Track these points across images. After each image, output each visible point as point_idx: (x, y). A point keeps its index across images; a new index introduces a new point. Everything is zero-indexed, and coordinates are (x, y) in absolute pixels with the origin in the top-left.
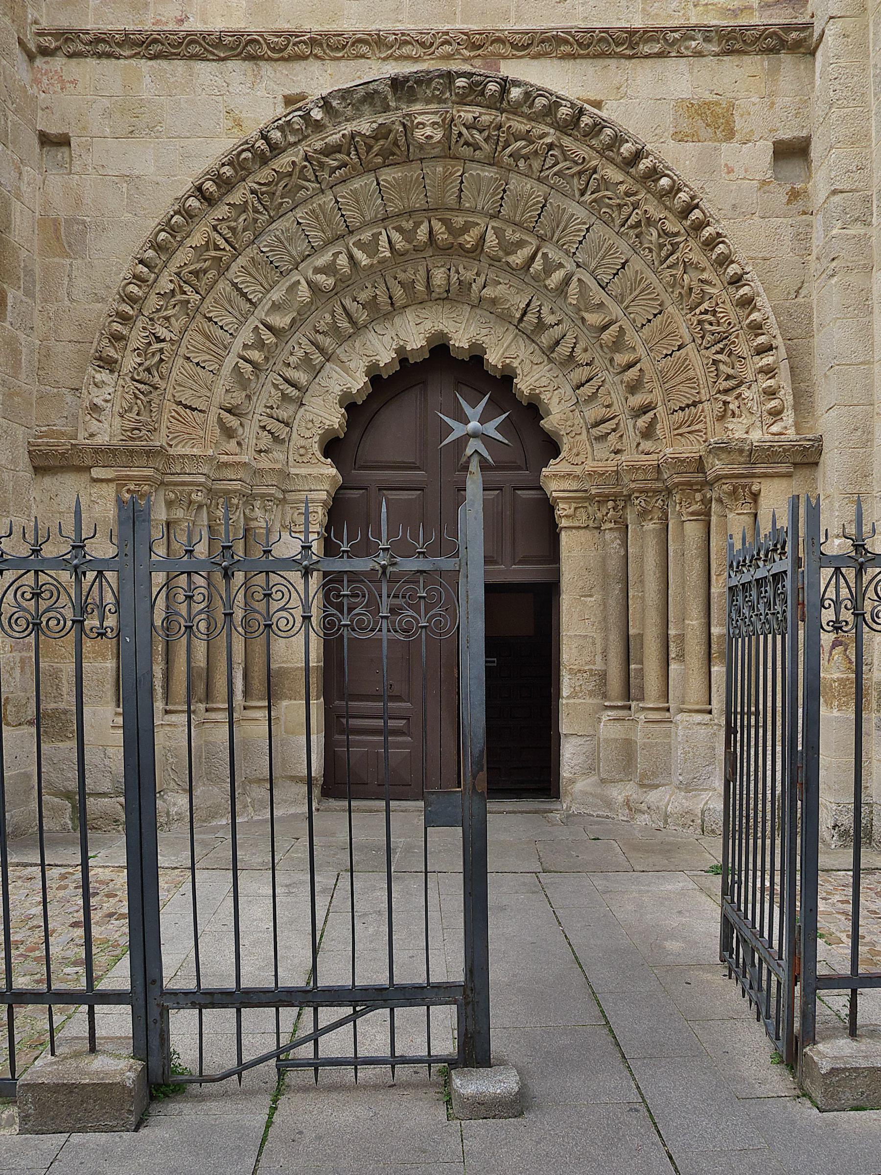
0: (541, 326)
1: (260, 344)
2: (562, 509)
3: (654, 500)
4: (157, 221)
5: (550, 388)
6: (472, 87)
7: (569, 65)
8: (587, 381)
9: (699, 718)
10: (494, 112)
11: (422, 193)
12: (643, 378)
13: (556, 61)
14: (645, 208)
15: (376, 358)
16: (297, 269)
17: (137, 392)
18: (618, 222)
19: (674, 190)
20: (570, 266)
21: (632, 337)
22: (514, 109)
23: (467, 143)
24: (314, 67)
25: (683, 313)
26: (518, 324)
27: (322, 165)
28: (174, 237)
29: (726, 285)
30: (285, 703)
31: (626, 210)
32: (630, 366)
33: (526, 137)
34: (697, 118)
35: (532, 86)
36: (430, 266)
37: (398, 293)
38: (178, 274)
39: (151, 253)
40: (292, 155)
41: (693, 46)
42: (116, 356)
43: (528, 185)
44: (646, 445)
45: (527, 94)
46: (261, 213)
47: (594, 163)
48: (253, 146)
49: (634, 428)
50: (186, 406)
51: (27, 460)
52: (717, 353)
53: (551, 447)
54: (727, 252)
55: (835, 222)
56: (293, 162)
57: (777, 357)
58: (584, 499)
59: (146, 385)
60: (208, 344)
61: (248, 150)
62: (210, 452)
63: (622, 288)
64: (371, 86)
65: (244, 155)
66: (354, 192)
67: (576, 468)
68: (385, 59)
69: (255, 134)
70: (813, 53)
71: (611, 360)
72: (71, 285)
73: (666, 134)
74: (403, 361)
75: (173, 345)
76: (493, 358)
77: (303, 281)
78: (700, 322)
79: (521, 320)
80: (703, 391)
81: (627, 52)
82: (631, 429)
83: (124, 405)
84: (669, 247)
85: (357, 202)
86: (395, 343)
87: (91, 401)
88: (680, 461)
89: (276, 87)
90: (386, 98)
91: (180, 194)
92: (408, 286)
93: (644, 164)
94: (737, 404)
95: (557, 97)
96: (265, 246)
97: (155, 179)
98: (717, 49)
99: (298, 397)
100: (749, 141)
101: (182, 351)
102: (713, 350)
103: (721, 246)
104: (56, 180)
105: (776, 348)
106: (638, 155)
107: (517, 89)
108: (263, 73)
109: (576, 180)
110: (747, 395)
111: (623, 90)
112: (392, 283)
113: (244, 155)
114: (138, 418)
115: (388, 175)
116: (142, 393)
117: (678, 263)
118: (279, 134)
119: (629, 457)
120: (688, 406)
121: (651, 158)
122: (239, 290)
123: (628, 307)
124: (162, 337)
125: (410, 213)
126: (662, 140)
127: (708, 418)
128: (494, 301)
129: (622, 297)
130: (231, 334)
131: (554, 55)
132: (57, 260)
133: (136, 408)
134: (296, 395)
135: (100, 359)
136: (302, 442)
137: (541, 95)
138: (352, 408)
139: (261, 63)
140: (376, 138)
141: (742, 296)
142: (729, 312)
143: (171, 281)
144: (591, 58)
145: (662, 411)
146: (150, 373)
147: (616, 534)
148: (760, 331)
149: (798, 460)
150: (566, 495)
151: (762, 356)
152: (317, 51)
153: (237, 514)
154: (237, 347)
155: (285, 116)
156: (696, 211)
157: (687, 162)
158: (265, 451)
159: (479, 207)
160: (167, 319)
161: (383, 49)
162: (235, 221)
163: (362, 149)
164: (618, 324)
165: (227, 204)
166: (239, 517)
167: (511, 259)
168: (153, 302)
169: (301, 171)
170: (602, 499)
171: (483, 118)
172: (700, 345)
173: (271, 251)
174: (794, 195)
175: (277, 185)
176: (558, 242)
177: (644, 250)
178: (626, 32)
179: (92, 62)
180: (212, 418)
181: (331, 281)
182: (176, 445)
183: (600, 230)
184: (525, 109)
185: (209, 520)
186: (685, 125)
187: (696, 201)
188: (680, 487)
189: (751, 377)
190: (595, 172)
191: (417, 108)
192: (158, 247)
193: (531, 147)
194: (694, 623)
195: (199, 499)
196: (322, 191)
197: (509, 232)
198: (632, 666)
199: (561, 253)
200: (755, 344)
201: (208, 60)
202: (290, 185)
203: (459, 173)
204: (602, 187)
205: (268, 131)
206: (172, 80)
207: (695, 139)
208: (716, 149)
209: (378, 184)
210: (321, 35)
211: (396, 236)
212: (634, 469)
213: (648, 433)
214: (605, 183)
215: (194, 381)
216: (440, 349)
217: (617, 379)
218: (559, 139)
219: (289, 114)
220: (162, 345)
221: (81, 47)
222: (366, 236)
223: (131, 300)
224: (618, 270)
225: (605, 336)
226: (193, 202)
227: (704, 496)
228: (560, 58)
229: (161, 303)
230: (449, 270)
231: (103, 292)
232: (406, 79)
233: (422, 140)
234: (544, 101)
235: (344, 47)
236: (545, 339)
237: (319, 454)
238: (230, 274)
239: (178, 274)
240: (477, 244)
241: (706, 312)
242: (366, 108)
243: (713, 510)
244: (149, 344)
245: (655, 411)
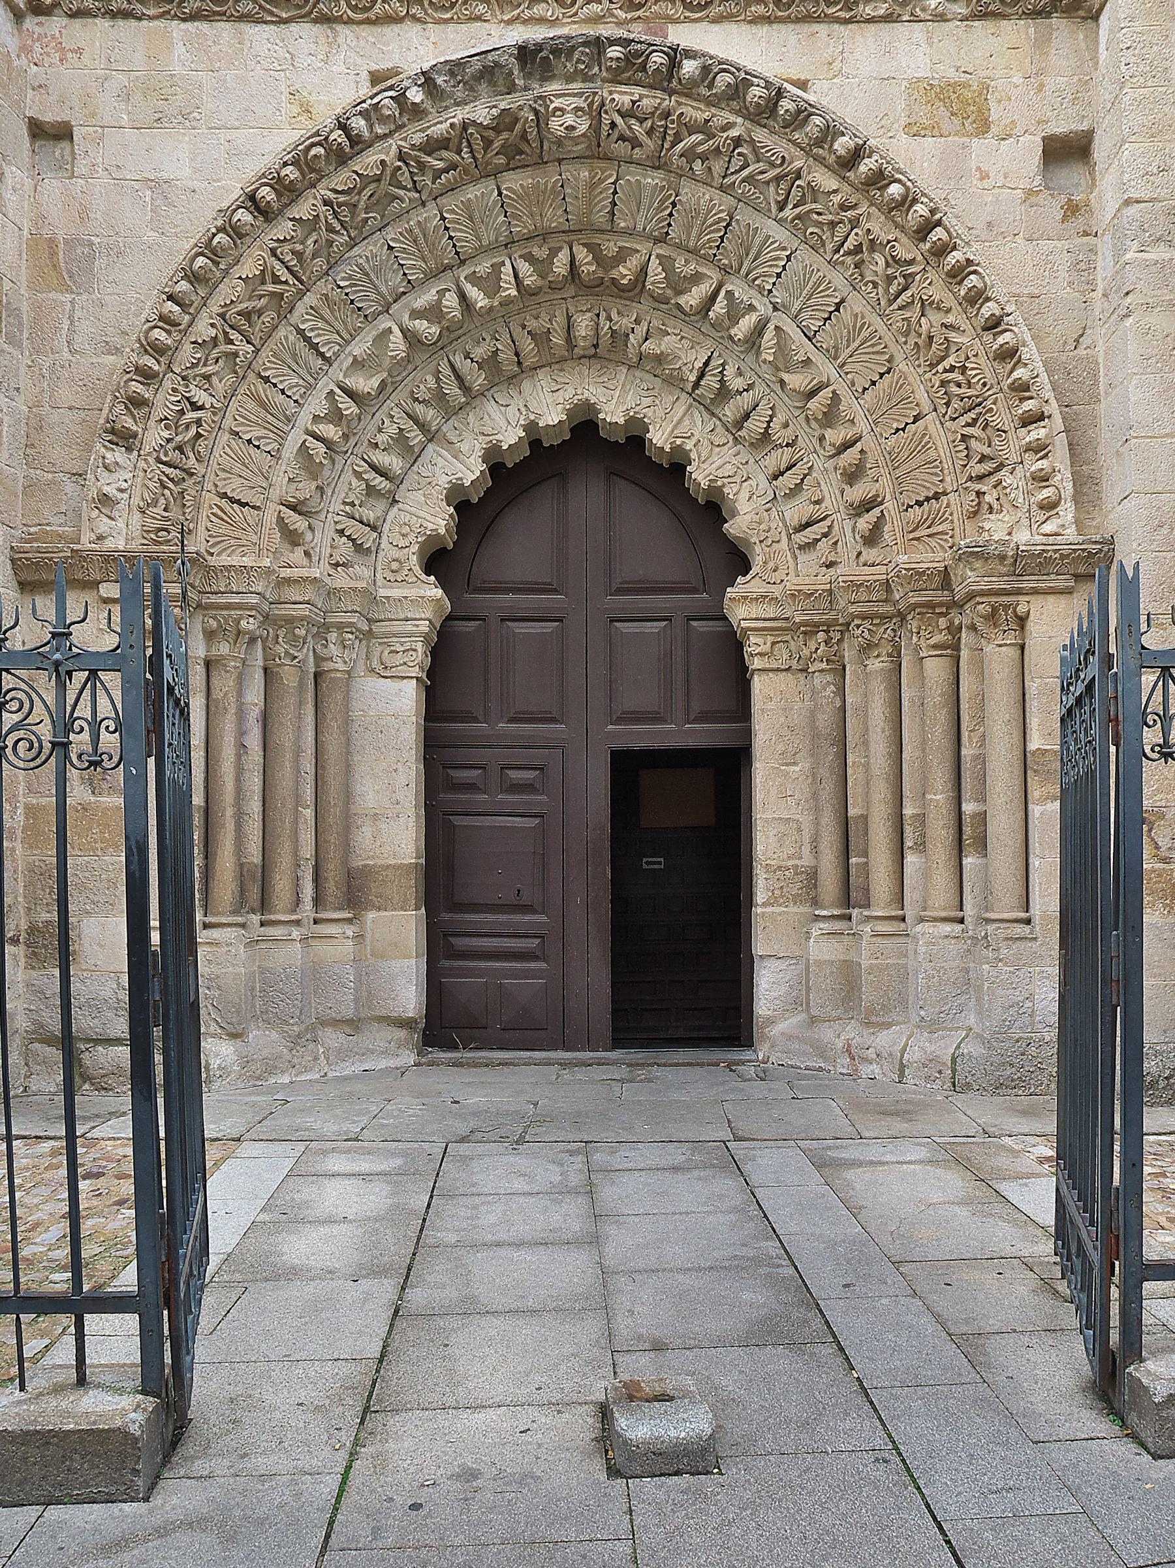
0: (724, 393)
1: (336, 416)
2: (755, 645)
3: (882, 630)
4: (193, 241)
5: (737, 479)
6: (629, 59)
7: (763, 30)
8: (788, 468)
9: (947, 928)
10: (659, 93)
11: (560, 207)
12: (865, 462)
13: (745, 27)
14: (867, 226)
15: (496, 437)
16: (387, 311)
17: (165, 479)
18: (830, 247)
19: (907, 201)
20: (763, 307)
21: (849, 405)
22: (688, 90)
23: (622, 138)
24: (411, 30)
25: (921, 370)
26: (693, 391)
27: (422, 166)
28: (217, 264)
29: (979, 331)
30: (371, 915)
31: (841, 230)
32: (847, 445)
33: (704, 128)
35: (711, 57)
36: (572, 310)
37: (528, 346)
38: (222, 316)
39: (184, 286)
40: (380, 152)
41: (933, 7)
42: (135, 428)
43: (707, 197)
44: (870, 554)
45: (706, 69)
46: (337, 233)
47: (798, 164)
48: (326, 139)
49: (853, 531)
50: (233, 501)
51: (10, 572)
52: (968, 425)
53: (738, 561)
54: (980, 285)
55: (1129, 243)
56: (383, 162)
57: (1051, 429)
58: (784, 629)
59: (178, 468)
60: (263, 413)
61: (319, 144)
62: (267, 562)
63: (836, 339)
65: (313, 152)
66: (467, 205)
67: (773, 588)
68: (509, 22)
69: (330, 122)
70: (1096, 17)
71: (822, 439)
72: (72, 330)
73: (896, 126)
74: (535, 444)
75: (214, 414)
76: (659, 437)
77: (396, 329)
78: (943, 383)
79: (696, 385)
80: (948, 479)
81: (842, 14)
82: (849, 533)
83: (146, 496)
84: (901, 280)
85: (471, 218)
86: (523, 417)
87: (100, 490)
88: (918, 573)
89: (359, 61)
90: (511, 73)
91: (225, 205)
92: (541, 338)
93: (867, 166)
94: (995, 495)
95: (747, 73)
96: (343, 279)
97: (190, 184)
98: (964, 11)
99: (389, 491)
100: (1010, 136)
101: (228, 422)
102: (962, 421)
103: (972, 277)
104: (52, 186)
105: (1049, 417)
106: (857, 154)
107: (693, 62)
108: (341, 40)
109: (772, 189)
110: (1008, 481)
111: (837, 65)
112: (517, 331)
113: (313, 152)
114: (166, 514)
115: (514, 182)
116: (172, 480)
117: (913, 302)
118: (363, 122)
119: (847, 570)
120: (928, 499)
122: (307, 340)
123: (843, 365)
124: (200, 403)
125: (544, 236)
126: (890, 134)
127: (955, 515)
128: (660, 359)
129: (836, 351)
130: (296, 401)
131: (742, 17)
132: (53, 295)
133: (162, 501)
134: (386, 488)
135: (113, 431)
136: (396, 553)
137: (724, 71)
138: (465, 507)
139: (339, 28)
140: (497, 130)
141: (1001, 346)
142: (983, 368)
143: (212, 325)
144: (792, 22)
145: (891, 508)
146: (182, 453)
147: (829, 678)
148: (1027, 394)
149: (1081, 570)
150: (760, 624)
151: (1029, 428)
153: (305, 650)
154: (304, 419)
155: (372, 98)
156: (938, 229)
157: (925, 165)
158: (343, 565)
159: (640, 228)
160: (207, 377)
161: (507, 8)
162: (302, 243)
163: (478, 145)
164: (830, 388)
165: (291, 220)
166: (307, 655)
167: (682, 300)
168: (187, 353)
169: (393, 175)
170: (810, 630)
171: (645, 101)
172: (944, 416)
174: (1072, 210)
175: (359, 193)
176: (747, 275)
177: (866, 285)
179: (102, 24)
180: (270, 517)
181: (435, 330)
182: (219, 554)
183: (805, 255)
184: (703, 91)
185: (265, 660)
187: (937, 217)
188: (918, 610)
189: (1015, 458)
190: (799, 177)
191: (553, 87)
192: (194, 278)
193: (711, 142)
194: (938, 797)
195: (251, 627)
196: (423, 204)
197: (679, 263)
198: (853, 860)
199: (753, 292)
200: (1020, 412)
201: (266, 22)
202: (380, 192)
203: (612, 180)
204: (809, 198)
205: (348, 119)
206: (214, 49)
208: (964, 146)
209: (500, 194)
211: (524, 268)
212: (854, 586)
213: (872, 538)
214: (813, 192)
215: (244, 464)
216: (584, 427)
217: (830, 464)
218: (749, 131)
219: (376, 94)
220: (199, 414)
222: (483, 267)
223: (157, 350)
224: (831, 313)
225: (813, 404)
226: (243, 216)
227: (952, 623)
228: (750, 22)
229: (198, 356)
230: (598, 315)
231: (118, 341)
232: (539, 47)
233: (561, 131)
234: (728, 78)
236: (730, 411)
237: (418, 570)
238: (294, 318)
240: (637, 280)
241: (952, 369)
242: (483, 87)
243: (963, 641)
244: (182, 412)
245: (882, 507)
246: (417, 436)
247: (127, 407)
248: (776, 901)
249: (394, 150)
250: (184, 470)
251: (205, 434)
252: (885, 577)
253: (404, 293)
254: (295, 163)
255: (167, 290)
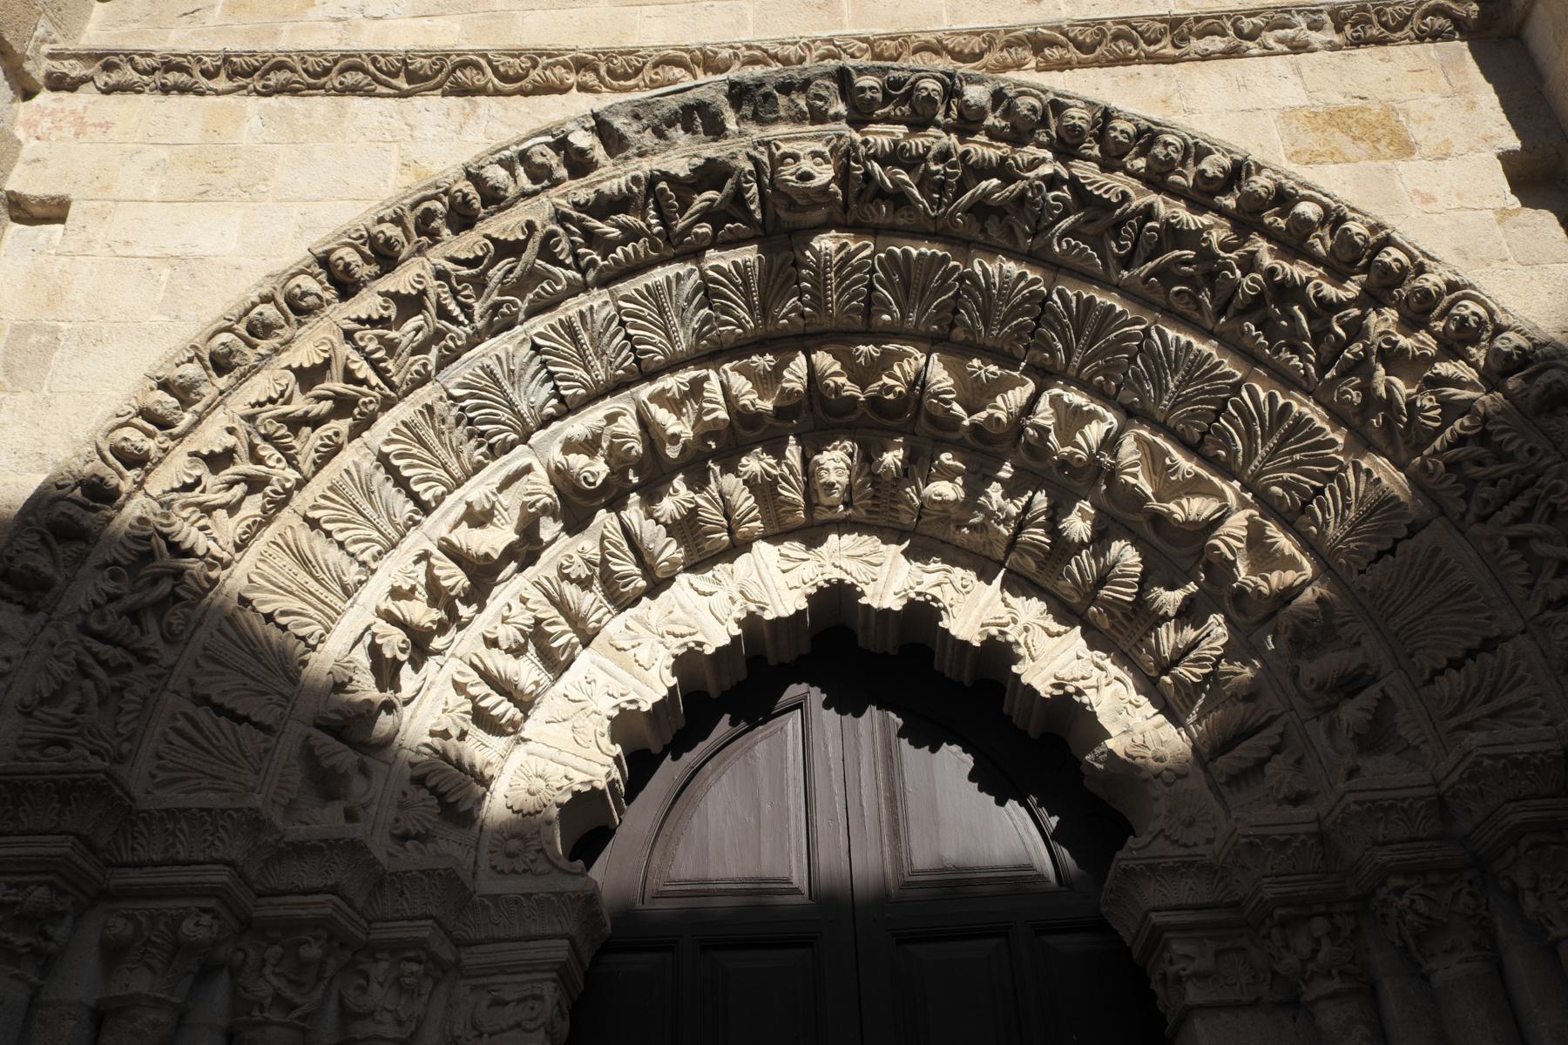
2: (1184, 956)
15: (695, 638)
17: (88, 660)
34: (1330, 130)
45: (998, 96)
46: (455, 321)
50: (219, 710)
60: (303, 577)
61: (436, 197)
64: (689, 94)
81: (1170, 51)
85: (662, 312)
86: (737, 607)
89: (505, 130)
92: (763, 489)
95: (1056, 94)
96: (461, 386)
108: (482, 111)
111: (1176, 101)
116: (103, 664)
121: (1265, 173)
122: (393, 471)
124: (187, 545)
133: (73, 699)
143: (231, 431)
152: (590, 78)
154: (374, 594)
155: (517, 144)
158: (417, 837)
160: (208, 510)
172: (1463, 515)
173: (472, 396)
178: (1162, 21)
186: (1310, 141)
193: (1012, 187)
207: (1336, 158)
210: (595, 54)
216: (835, 600)
221: (136, 77)
222: (672, 383)
229: (197, 472)
232: (760, 84)
235: (638, 71)
239: (251, 419)
242: (677, 133)
245: (1382, 683)
246: (564, 633)
247: (43, 540)
249: (548, 210)
250: (134, 652)
251: (189, 596)
253: (551, 419)
254: (398, 220)
255: (160, 374)
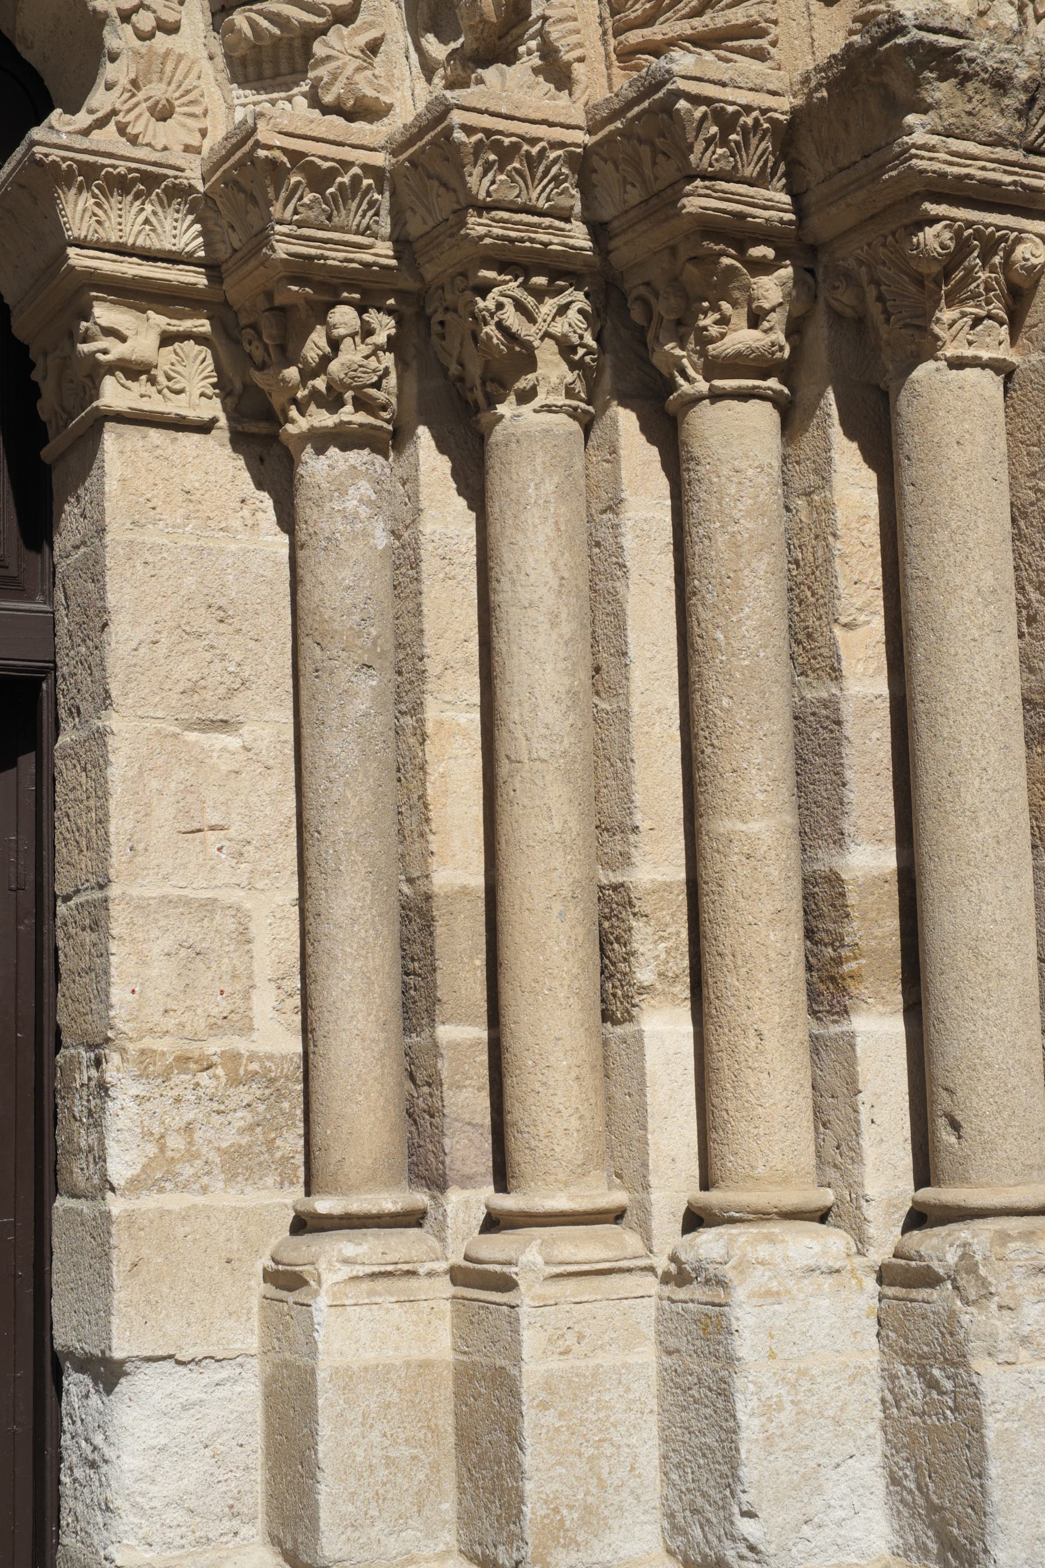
150: (131, 268)
248: (171, 1175)
252: (581, 137)
